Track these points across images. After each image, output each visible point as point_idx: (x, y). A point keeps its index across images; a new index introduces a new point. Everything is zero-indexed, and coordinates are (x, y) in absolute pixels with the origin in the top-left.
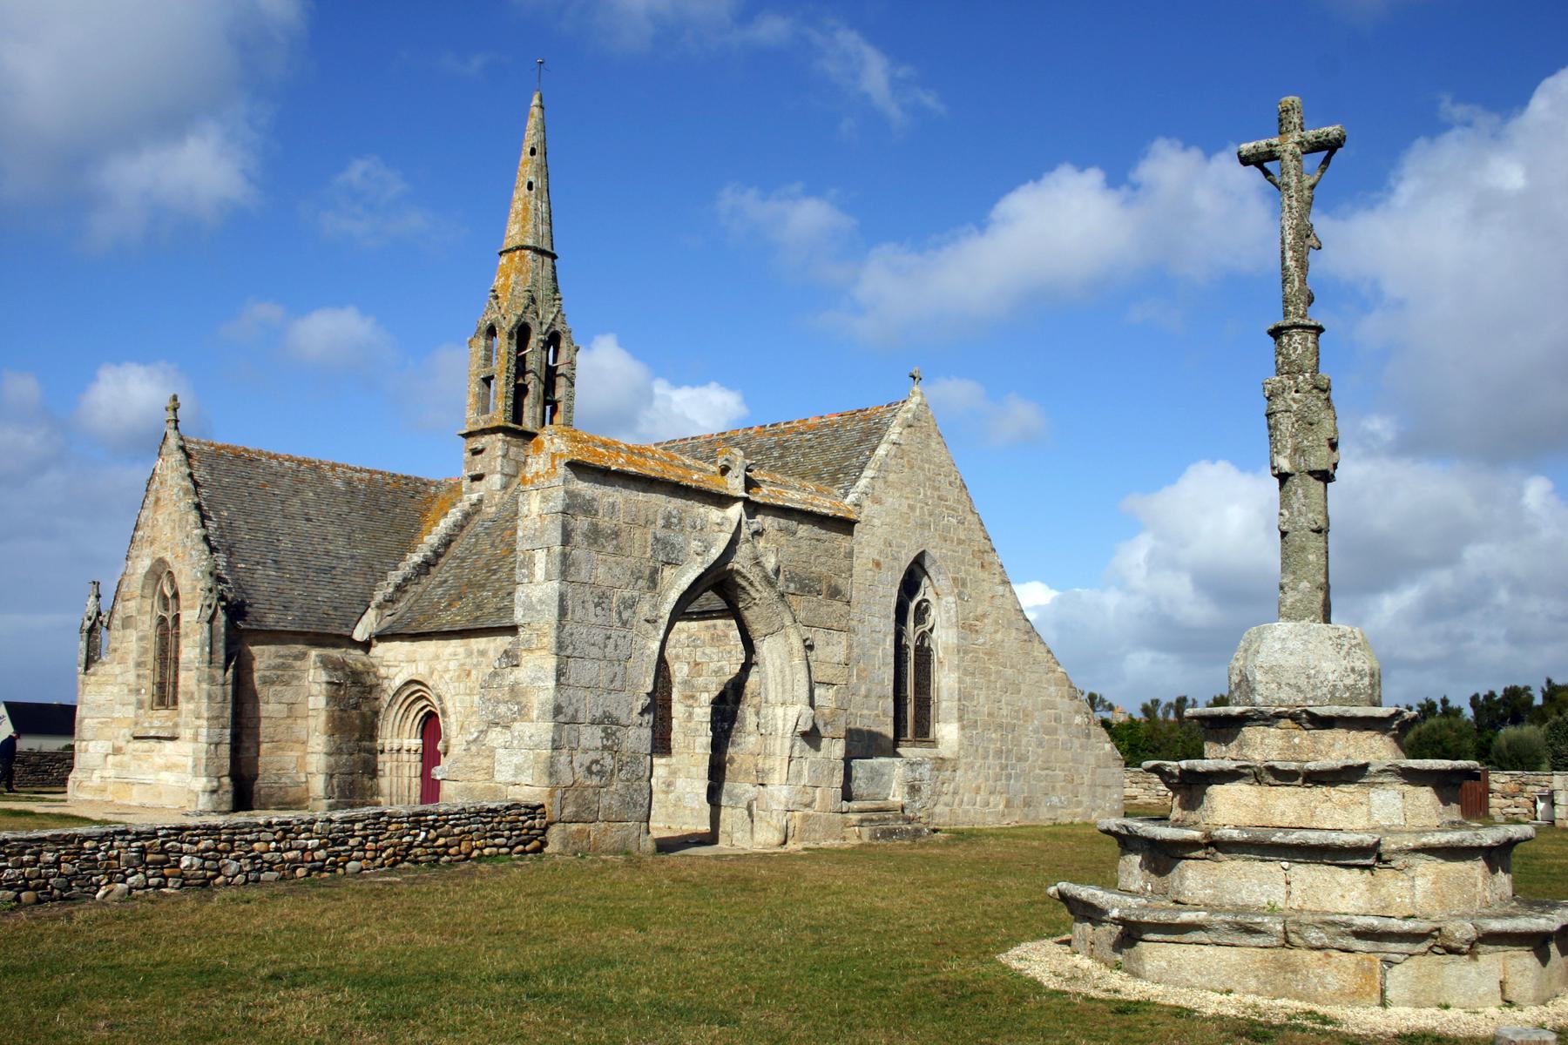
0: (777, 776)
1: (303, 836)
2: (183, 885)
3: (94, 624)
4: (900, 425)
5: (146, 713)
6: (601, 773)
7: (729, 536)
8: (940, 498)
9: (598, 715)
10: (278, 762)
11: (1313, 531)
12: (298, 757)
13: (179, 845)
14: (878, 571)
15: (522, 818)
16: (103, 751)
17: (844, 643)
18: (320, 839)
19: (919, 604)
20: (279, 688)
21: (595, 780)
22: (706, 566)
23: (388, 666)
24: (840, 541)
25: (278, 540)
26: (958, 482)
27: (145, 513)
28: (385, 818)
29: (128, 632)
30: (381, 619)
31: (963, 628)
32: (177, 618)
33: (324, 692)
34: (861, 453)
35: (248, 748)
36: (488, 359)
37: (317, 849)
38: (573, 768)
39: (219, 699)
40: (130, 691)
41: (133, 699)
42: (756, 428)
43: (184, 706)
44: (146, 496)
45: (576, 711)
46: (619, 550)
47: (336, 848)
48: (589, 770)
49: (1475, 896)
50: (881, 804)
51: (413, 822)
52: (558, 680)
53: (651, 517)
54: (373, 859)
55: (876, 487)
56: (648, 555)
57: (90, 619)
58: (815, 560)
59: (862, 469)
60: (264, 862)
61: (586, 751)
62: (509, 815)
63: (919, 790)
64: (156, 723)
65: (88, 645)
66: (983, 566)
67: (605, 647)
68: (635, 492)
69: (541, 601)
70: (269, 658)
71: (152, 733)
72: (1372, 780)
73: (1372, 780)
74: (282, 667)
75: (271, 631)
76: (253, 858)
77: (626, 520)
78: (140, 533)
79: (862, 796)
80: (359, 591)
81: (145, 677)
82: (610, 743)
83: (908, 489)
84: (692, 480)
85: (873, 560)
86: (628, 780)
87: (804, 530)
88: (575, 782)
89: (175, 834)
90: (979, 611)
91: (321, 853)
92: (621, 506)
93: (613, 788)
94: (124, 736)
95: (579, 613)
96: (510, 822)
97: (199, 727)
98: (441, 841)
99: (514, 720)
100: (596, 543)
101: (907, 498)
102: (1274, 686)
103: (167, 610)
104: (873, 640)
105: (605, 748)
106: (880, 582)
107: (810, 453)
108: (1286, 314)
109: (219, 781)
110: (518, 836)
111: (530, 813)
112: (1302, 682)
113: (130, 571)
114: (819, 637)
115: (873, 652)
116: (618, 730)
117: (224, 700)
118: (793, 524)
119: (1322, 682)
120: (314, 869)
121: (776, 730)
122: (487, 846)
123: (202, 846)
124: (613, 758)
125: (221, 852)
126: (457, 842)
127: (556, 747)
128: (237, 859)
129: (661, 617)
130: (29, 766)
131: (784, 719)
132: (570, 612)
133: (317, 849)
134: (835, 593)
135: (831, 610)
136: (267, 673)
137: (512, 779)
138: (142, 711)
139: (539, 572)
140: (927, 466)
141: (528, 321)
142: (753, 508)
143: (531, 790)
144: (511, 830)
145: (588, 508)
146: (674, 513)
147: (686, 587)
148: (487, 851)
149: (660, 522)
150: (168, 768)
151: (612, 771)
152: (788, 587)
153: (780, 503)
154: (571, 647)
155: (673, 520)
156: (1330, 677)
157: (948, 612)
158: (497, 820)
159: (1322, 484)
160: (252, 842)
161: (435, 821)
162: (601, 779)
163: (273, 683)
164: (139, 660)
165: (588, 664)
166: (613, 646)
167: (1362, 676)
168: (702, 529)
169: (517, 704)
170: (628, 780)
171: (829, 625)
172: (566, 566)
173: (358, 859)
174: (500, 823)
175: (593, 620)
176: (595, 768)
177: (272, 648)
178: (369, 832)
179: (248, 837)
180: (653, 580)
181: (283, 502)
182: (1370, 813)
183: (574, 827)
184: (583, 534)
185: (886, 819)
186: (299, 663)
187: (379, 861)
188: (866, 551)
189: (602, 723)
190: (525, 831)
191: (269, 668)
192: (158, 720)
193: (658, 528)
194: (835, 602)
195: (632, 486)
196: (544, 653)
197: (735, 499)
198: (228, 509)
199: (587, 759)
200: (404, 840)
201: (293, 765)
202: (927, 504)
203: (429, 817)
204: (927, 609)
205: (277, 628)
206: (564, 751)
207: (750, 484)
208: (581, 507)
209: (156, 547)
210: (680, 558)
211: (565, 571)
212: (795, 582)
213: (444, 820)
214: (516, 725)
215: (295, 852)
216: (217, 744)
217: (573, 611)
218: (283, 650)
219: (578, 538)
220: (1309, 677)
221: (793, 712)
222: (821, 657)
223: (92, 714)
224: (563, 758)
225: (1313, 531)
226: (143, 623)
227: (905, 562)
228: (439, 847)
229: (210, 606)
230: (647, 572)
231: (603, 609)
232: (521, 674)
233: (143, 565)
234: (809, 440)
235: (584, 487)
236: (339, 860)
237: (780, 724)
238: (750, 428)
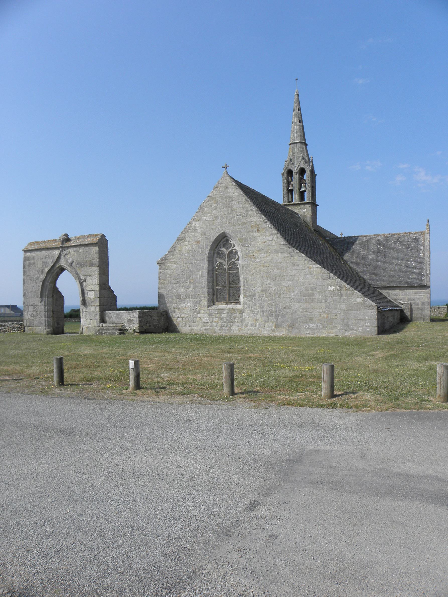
6: (34, 316)
38: (28, 316)
48: (31, 316)
52: (24, 297)
56: (41, 266)
58: (85, 257)
82: (35, 310)
85: (196, 241)
86: (39, 318)
88: (28, 318)
105: (34, 311)
141: (290, 168)
152: (76, 266)
170: (39, 318)
171: (91, 274)
185: (108, 329)
199: (31, 313)
212: (78, 264)
222: (89, 283)
235: (28, 254)
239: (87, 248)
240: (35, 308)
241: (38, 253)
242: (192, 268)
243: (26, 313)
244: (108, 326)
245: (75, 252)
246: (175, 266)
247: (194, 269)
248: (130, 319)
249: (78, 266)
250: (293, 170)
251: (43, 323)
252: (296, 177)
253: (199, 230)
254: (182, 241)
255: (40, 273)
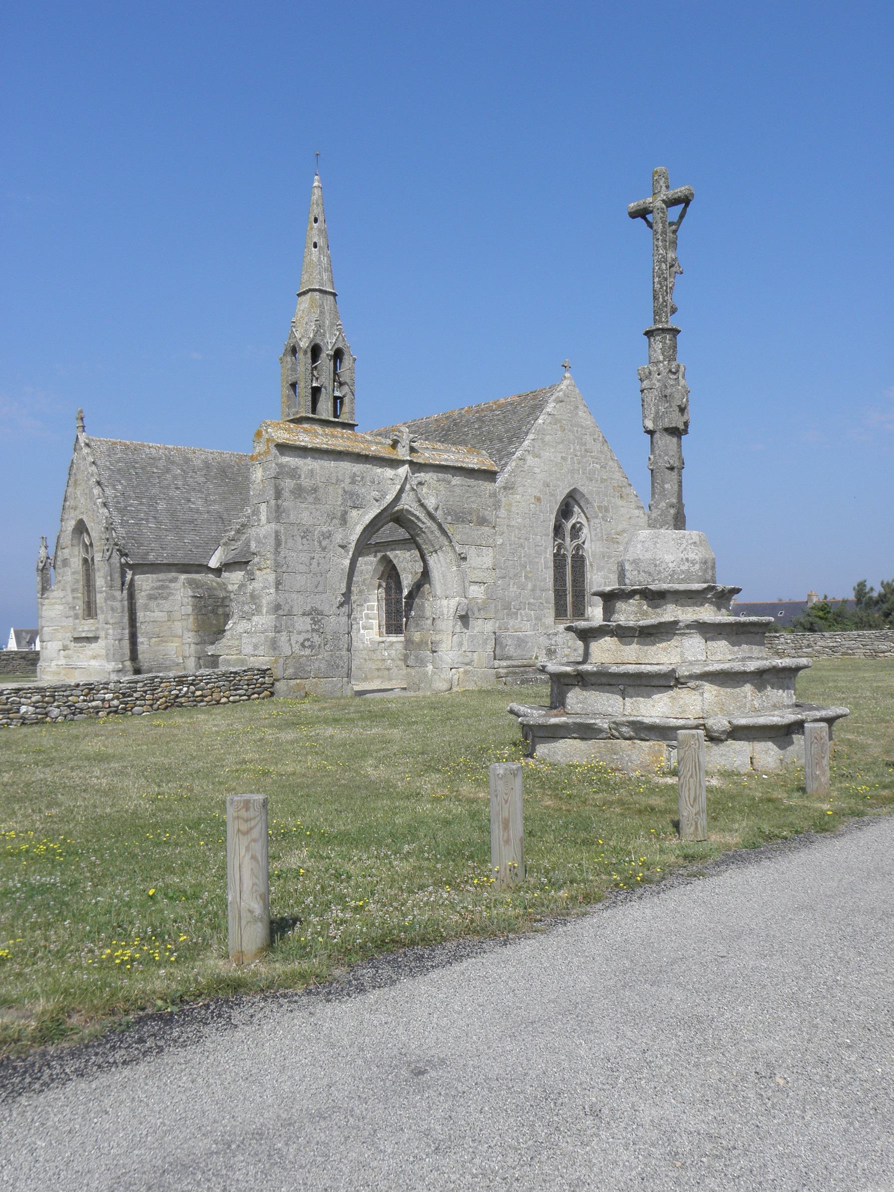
0: (444, 645)
1: (102, 692)
2: (23, 724)
3: (45, 565)
4: (554, 401)
5: (80, 622)
6: (312, 647)
7: (399, 487)
8: (586, 451)
9: (307, 609)
10: (164, 650)
11: (668, 468)
12: (177, 647)
13: (18, 699)
14: (538, 504)
15: (255, 677)
16: (57, 648)
17: (491, 555)
18: (114, 693)
19: (574, 526)
20: (161, 602)
21: (307, 652)
22: (382, 508)
23: (233, 584)
24: (487, 487)
25: (156, 503)
26: (601, 438)
27: (70, 489)
28: (158, 680)
29: (65, 569)
30: (228, 553)
31: (606, 540)
32: (93, 559)
33: (191, 603)
34: (528, 422)
35: (142, 643)
36: (294, 370)
37: (113, 699)
38: (291, 645)
39: (119, 611)
40: (70, 608)
41: (72, 613)
42: (466, 408)
43: (101, 617)
44: (69, 479)
45: (292, 607)
46: (317, 500)
47: (126, 699)
48: (303, 645)
49: (745, 704)
50: (525, 662)
51: (177, 682)
53: (341, 478)
54: (151, 705)
55: (536, 446)
56: (339, 503)
57: (42, 562)
59: (527, 433)
60: (76, 708)
61: (299, 633)
62: (246, 675)
63: (555, 652)
64: (86, 628)
65: (42, 579)
66: (621, 497)
67: (311, 564)
68: (329, 462)
69: (265, 537)
70: (152, 582)
71: (84, 635)
72: (683, 631)
73: (683, 631)
74: (162, 587)
75: (152, 564)
76: (69, 706)
77: (322, 480)
78: (68, 503)
79: (511, 657)
80: (213, 534)
81: (78, 598)
82: (317, 627)
83: (561, 446)
84: (371, 451)
85: (535, 497)
86: (331, 651)
87: (456, 480)
89: (14, 693)
90: (620, 528)
91: (116, 702)
92: (318, 471)
93: (320, 657)
94: (69, 638)
95: (290, 543)
96: (248, 680)
97: (108, 629)
98: (198, 693)
99: (253, 614)
100: (300, 496)
101: (561, 452)
102: (635, 573)
103: (88, 553)
104: (536, 552)
105: (313, 630)
106: (541, 511)
107: (498, 424)
108: (655, 321)
109: (122, 664)
110: (253, 689)
111: (261, 674)
112: (651, 569)
113: (64, 529)
114: (471, 552)
115: (537, 560)
116: (322, 618)
117: (123, 611)
118: (448, 476)
119: (664, 569)
120: (110, 712)
121: (443, 615)
122: (231, 696)
123: (34, 699)
124: (319, 637)
125: (47, 703)
126: (210, 694)
127: (278, 630)
128: (58, 707)
129: (350, 543)
130: (28, 660)
131: (448, 607)
132: (283, 543)
133: (113, 699)
134: (482, 521)
135: (480, 533)
136: (152, 592)
137: (253, 653)
138: (77, 621)
139: (263, 518)
140: (575, 429)
142: (416, 467)
143: (262, 661)
144: (248, 685)
145: (294, 473)
146: (358, 473)
147: (368, 522)
148: (231, 698)
149: (348, 480)
150: (94, 658)
151: (319, 645)
152: (446, 519)
153: (437, 463)
154: (285, 566)
155: (357, 478)
156: (670, 565)
157: (595, 530)
158: (237, 679)
159: (675, 440)
160: (68, 696)
161: (194, 680)
162: (312, 651)
163: (156, 599)
164: (73, 587)
165: (299, 577)
166: (316, 564)
167: (693, 563)
168: (379, 483)
169: (255, 604)
170: (331, 651)
172: (278, 514)
173: (140, 706)
174: (240, 681)
175: (301, 547)
176: (307, 644)
177: (154, 576)
178: (146, 688)
179: (65, 694)
180: (344, 520)
181: (159, 477)
182: (682, 653)
183: (293, 682)
184: (290, 491)
185: (526, 672)
186: (173, 584)
187: (155, 706)
188: (529, 491)
189: (311, 614)
190: (258, 685)
191: (153, 588)
192: (86, 627)
193: (346, 485)
194: (483, 527)
195: (325, 458)
196: (268, 570)
197: (403, 462)
198: (122, 484)
199: (301, 639)
200: (172, 693)
201: (174, 652)
202: (576, 456)
203: (189, 678)
204: (580, 529)
205: (156, 562)
206: (283, 633)
207: (412, 450)
208: (288, 473)
209: (77, 512)
210: (364, 504)
211: (278, 516)
213: (200, 680)
214: (255, 618)
215: (97, 702)
216: (120, 640)
217: (286, 542)
218: (162, 576)
219: (286, 494)
220: (656, 566)
221: (453, 602)
222: (474, 565)
223: (48, 624)
224: (283, 637)
225: (668, 468)
226: (74, 563)
227: (560, 498)
228: (197, 697)
229: (108, 550)
230: (339, 514)
231: (308, 540)
232: (257, 585)
233: (71, 524)
234: (498, 415)
236: (128, 706)
237: (445, 611)
238: (462, 409)
239: (472, 482)
240: (319, 621)
241: (331, 465)
242: (529, 549)
243: (282, 639)
244: (514, 666)
245: (441, 482)
246: (500, 542)
247: (532, 552)
248: (550, 650)
249: (449, 518)
250: (324, 348)
251: (342, 667)
252: (325, 362)
253: (539, 477)
254: (511, 492)
255: (335, 521)
